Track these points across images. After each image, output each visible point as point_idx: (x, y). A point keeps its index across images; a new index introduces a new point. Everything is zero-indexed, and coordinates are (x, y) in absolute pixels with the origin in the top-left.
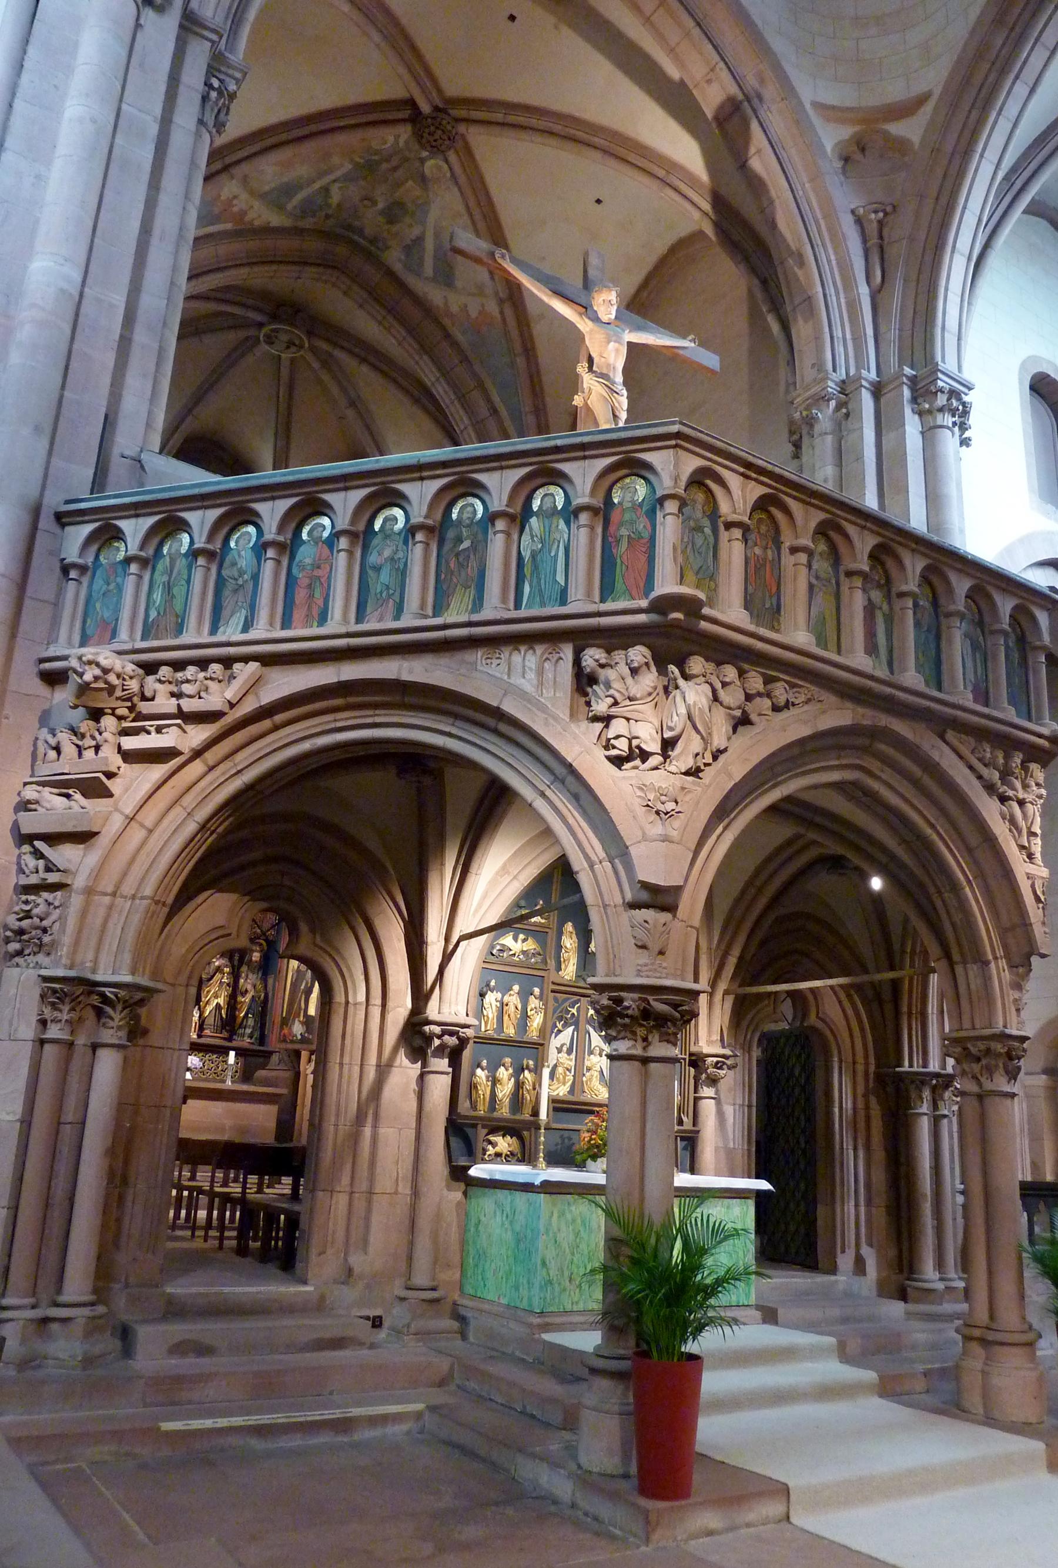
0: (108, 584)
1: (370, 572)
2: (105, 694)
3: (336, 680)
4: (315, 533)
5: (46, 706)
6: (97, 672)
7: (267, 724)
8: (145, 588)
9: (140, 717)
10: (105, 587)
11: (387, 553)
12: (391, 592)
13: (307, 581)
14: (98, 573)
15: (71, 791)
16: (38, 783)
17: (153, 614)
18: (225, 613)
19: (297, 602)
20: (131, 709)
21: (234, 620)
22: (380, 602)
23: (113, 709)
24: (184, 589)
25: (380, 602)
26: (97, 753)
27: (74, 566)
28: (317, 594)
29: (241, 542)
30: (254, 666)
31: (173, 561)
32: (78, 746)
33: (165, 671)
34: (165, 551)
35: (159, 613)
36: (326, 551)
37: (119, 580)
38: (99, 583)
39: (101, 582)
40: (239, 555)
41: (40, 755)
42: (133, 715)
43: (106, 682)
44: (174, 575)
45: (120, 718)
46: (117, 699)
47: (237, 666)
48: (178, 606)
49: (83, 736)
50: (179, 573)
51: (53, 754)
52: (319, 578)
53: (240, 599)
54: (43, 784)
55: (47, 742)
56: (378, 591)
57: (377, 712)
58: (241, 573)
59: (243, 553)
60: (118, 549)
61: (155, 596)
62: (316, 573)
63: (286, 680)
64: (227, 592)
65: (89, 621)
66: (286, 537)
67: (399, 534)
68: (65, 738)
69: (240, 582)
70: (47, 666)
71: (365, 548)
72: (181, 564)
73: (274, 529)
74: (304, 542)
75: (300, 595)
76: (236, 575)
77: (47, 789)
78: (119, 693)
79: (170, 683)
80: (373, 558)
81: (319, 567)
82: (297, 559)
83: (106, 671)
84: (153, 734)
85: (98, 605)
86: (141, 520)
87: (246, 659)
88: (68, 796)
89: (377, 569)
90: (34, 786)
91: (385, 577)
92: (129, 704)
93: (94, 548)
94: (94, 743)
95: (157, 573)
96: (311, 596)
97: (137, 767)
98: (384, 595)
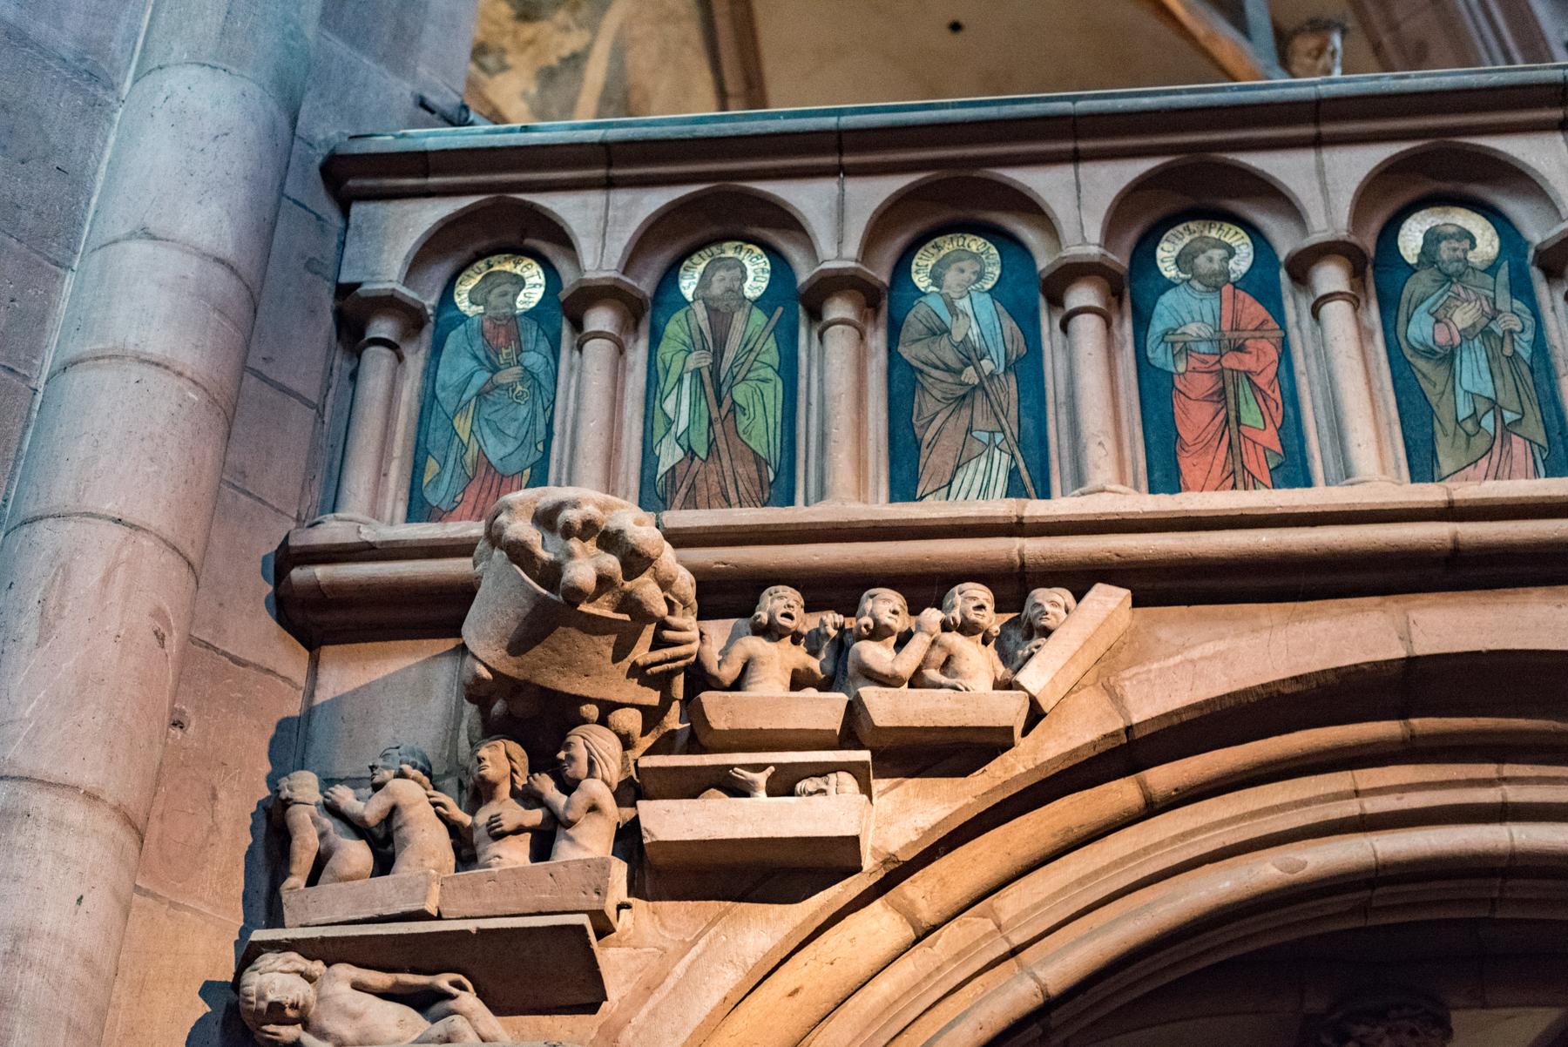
0: (495, 370)
1: (1421, 364)
2: (606, 645)
3: (1399, 652)
4: (1201, 260)
5: (294, 708)
6: (611, 563)
7: (1122, 793)
8: (636, 380)
9: (694, 745)
10: (480, 379)
11: (1464, 317)
12: (1509, 416)
13: (1205, 383)
14: (454, 339)
15: (443, 981)
16: (308, 949)
17: (670, 455)
18: (935, 461)
19: (1187, 434)
20: (652, 717)
21: (971, 476)
22: (1480, 443)
23: (608, 708)
24: (773, 392)
25: (1480, 443)
26: (542, 849)
27: (389, 304)
28: (1251, 415)
29: (951, 277)
30: (1108, 600)
31: (719, 318)
32: (454, 829)
33: (780, 602)
34: (688, 285)
35: (690, 453)
36: (1253, 311)
37: (534, 359)
38: (458, 365)
39: (468, 364)
40: (951, 306)
41: (303, 860)
42: (648, 741)
43: (629, 603)
44: (729, 355)
45: (627, 742)
46: (637, 672)
47: (1051, 600)
48: (760, 431)
49: (479, 793)
50: (747, 346)
51: (357, 854)
52: (1248, 375)
53: (980, 422)
54: (327, 951)
55: (333, 810)
56: (1464, 411)
57: (1509, 770)
58: (970, 355)
59: (964, 304)
60: (519, 282)
61: (669, 406)
62: (1231, 361)
63: (1221, 646)
64: (927, 404)
65: (432, 466)
66: (1120, 259)
67: (1492, 269)
68: (412, 794)
69: (970, 376)
70: (321, 572)
71: (1389, 305)
72: (750, 326)
73: (1094, 233)
74: (1171, 285)
75: (1195, 418)
76: (951, 358)
77: (346, 972)
78: (642, 653)
79: (796, 638)
80: (1420, 329)
81: (1240, 349)
82: (1157, 327)
83: (636, 561)
84: (762, 795)
85: (463, 425)
86: (621, 197)
87: (1079, 578)
88: (425, 1001)
89: (1447, 358)
90: (296, 960)
91: (1474, 375)
92: (652, 697)
93: (440, 272)
94: (536, 816)
95: (666, 350)
96: (1231, 423)
97: (680, 914)
98: (1488, 422)
